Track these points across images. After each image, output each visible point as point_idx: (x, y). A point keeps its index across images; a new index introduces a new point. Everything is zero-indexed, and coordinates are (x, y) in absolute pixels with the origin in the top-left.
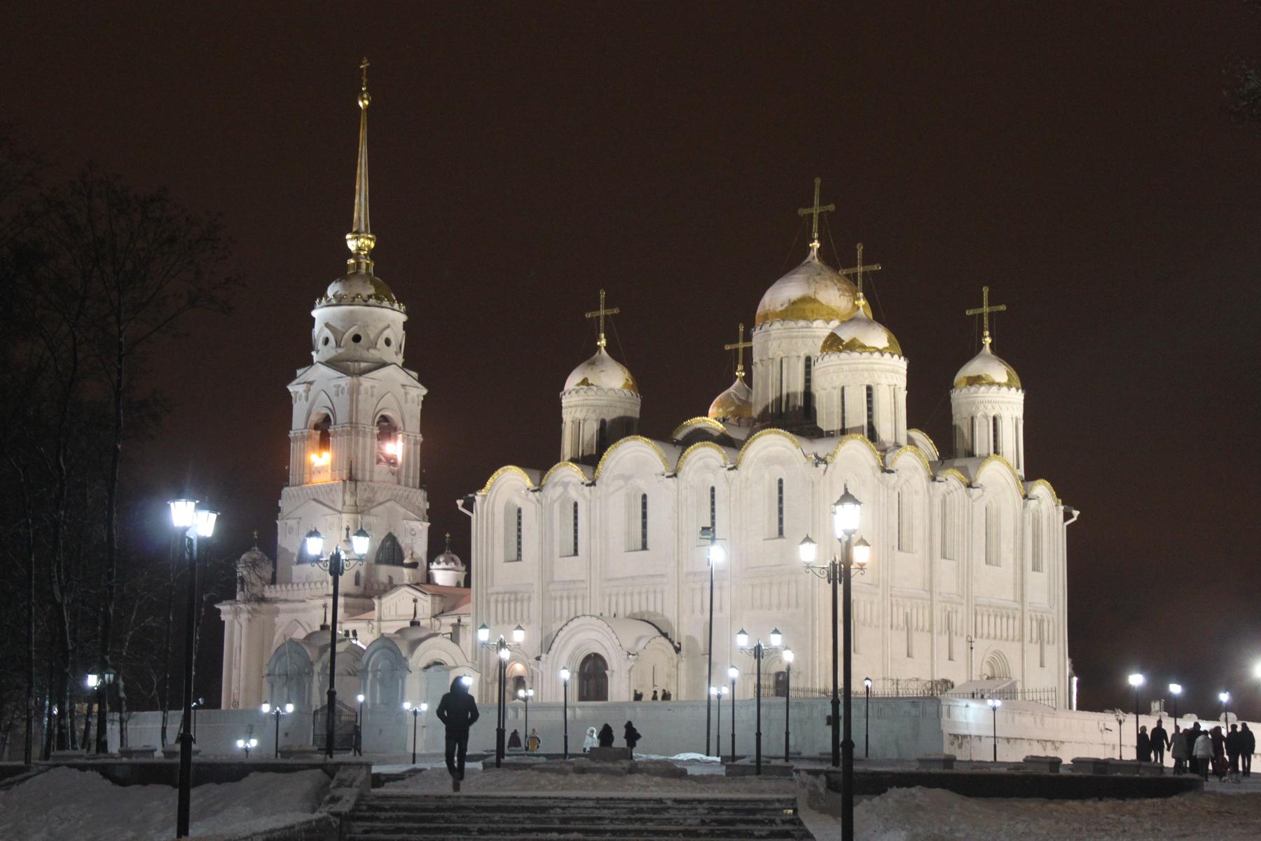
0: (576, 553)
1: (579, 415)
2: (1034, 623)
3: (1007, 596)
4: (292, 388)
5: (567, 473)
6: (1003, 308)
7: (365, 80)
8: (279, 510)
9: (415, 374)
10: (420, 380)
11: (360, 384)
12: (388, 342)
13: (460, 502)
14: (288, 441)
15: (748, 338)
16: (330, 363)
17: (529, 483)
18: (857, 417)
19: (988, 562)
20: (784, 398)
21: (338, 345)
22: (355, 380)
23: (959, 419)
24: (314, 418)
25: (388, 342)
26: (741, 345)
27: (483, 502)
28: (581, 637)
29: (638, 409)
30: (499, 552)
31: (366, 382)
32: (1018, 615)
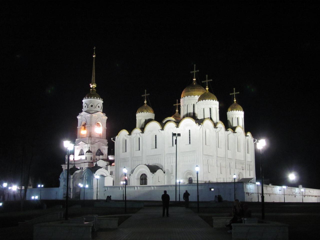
0: (139, 150)
1: (140, 118)
2: (248, 166)
3: (243, 159)
4: (78, 117)
5: (137, 131)
6: (238, 93)
7: (95, 51)
9: (105, 114)
11: (92, 116)
12: (99, 107)
13: (112, 139)
14: (77, 129)
15: (179, 102)
16: (85, 112)
17: (128, 133)
18: (207, 115)
19: (238, 151)
20: (188, 114)
21: (88, 107)
22: (91, 114)
23: (229, 118)
25: (99, 107)
26: (177, 104)
27: (117, 138)
28: (140, 170)
29: (154, 117)
30: (121, 150)
31: (94, 115)
32: (245, 164)
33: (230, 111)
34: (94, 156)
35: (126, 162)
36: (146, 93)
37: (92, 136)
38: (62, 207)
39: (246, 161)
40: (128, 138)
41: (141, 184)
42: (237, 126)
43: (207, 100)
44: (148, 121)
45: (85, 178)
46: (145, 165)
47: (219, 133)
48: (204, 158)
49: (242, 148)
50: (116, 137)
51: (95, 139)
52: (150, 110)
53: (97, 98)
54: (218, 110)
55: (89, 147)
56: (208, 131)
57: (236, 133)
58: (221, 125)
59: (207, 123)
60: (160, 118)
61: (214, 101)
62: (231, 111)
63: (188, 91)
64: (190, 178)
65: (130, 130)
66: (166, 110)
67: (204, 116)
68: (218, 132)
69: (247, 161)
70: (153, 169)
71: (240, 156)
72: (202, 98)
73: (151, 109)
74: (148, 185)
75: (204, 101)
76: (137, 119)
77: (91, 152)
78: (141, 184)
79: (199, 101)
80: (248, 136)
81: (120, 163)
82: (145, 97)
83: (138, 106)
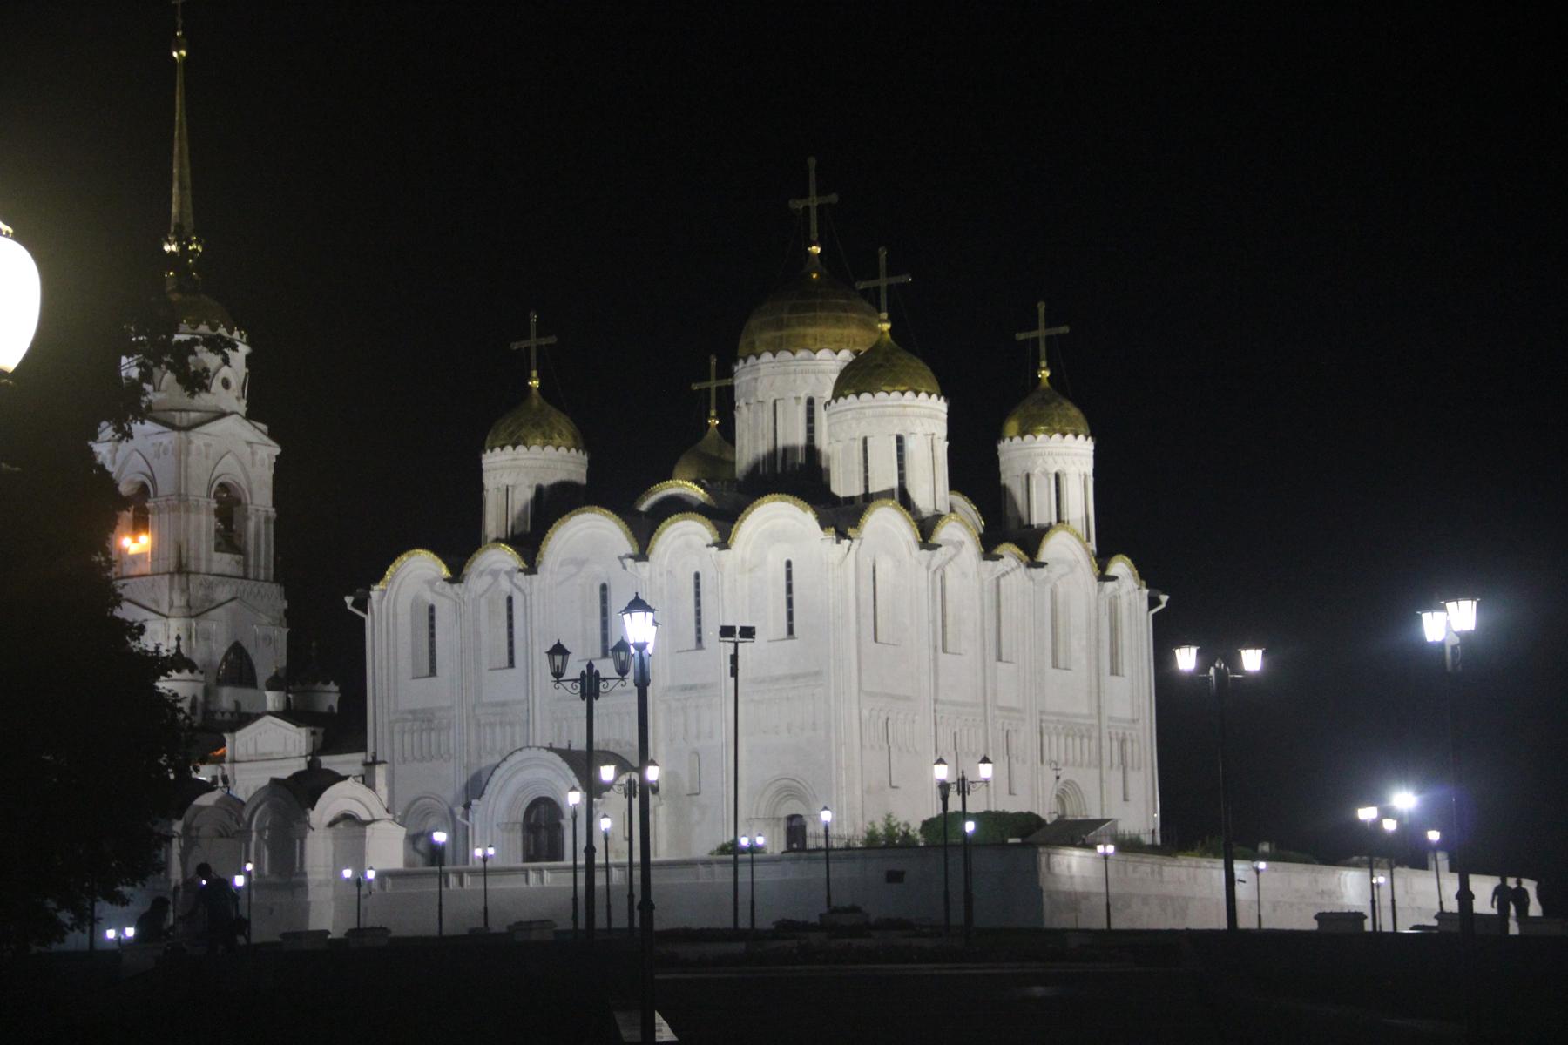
0: (511, 663)
1: (507, 479)
2: (1115, 744)
3: (1083, 708)
5: (498, 559)
6: (1065, 329)
7: (180, 22)
9: (264, 427)
10: (271, 435)
11: (190, 442)
17: (445, 572)
19: (1055, 666)
20: (780, 455)
22: (183, 434)
23: (1010, 476)
25: (226, 384)
26: (713, 384)
27: (380, 601)
28: (527, 775)
29: (584, 471)
30: (405, 664)
31: (198, 438)
32: (1095, 734)
33: (1017, 439)
34: (207, 692)
35: (433, 735)
36: (533, 333)
37: (193, 568)
39: (1105, 723)
40: (445, 600)
41: (528, 857)
42: (1054, 520)
43: (881, 395)
44: (553, 505)
45: (260, 832)
46: (550, 749)
47: (948, 569)
48: (865, 713)
49: (1078, 645)
50: (375, 592)
51: (210, 586)
52: (560, 434)
54: (942, 447)
55: (178, 638)
56: (885, 568)
57: (1043, 565)
58: (960, 530)
59: (885, 522)
60: (622, 483)
61: (923, 395)
62: (1022, 434)
63: (780, 325)
64: (791, 818)
65: (458, 549)
66: (659, 441)
67: (866, 479)
68: (942, 568)
69: (1111, 718)
71: (1069, 691)
72: (854, 381)
73: (563, 423)
75: (865, 396)
77: (192, 667)
79: (841, 400)
80: (1113, 578)
81: (397, 738)
82: (533, 355)
83: (496, 414)
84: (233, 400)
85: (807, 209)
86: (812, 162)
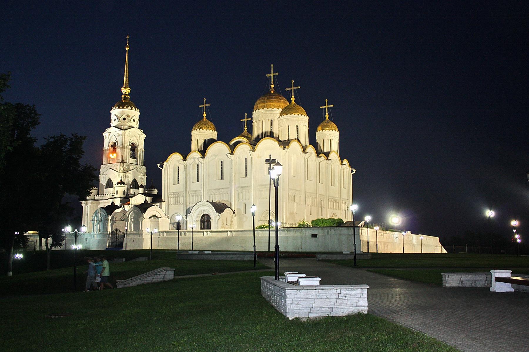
1: (198, 138)
4: (104, 134)
5: (195, 155)
8: (100, 172)
12: (134, 121)
13: (159, 165)
15: (250, 116)
16: (115, 127)
17: (182, 158)
18: (293, 136)
24: (111, 144)
25: (134, 121)
28: (202, 208)
34: (128, 189)
38: (124, 260)
40: (182, 165)
41: (201, 229)
43: (293, 115)
44: (208, 143)
45: (131, 219)
49: (336, 181)
50: (165, 163)
51: (129, 166)
53: (132, 108)
56: (294, 157)
57: (330, 160)
58: (311, 149)
59: (294, 145)
63: (264, 102)
65: (185, 152)
70: (220, 208)
72: (286, 111)
73: (211, 124)
74: (213, 228)
76: (193, 138)
77: (124, 184)
78: (201, 229)
81: (169, 199)
83: (195, 120)
84: (136, 124)
85: (271, 76)
86: (272, 65)
